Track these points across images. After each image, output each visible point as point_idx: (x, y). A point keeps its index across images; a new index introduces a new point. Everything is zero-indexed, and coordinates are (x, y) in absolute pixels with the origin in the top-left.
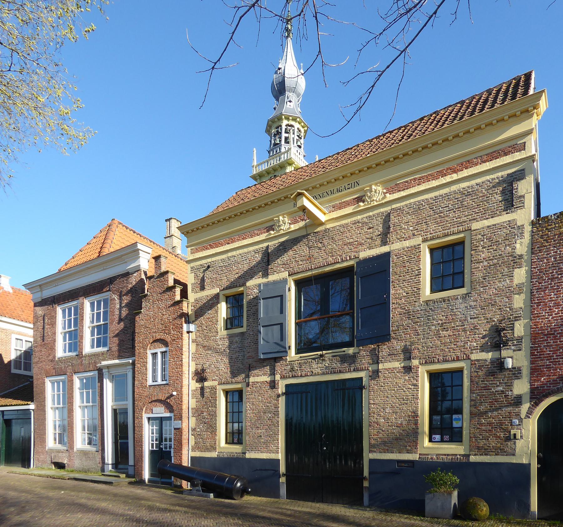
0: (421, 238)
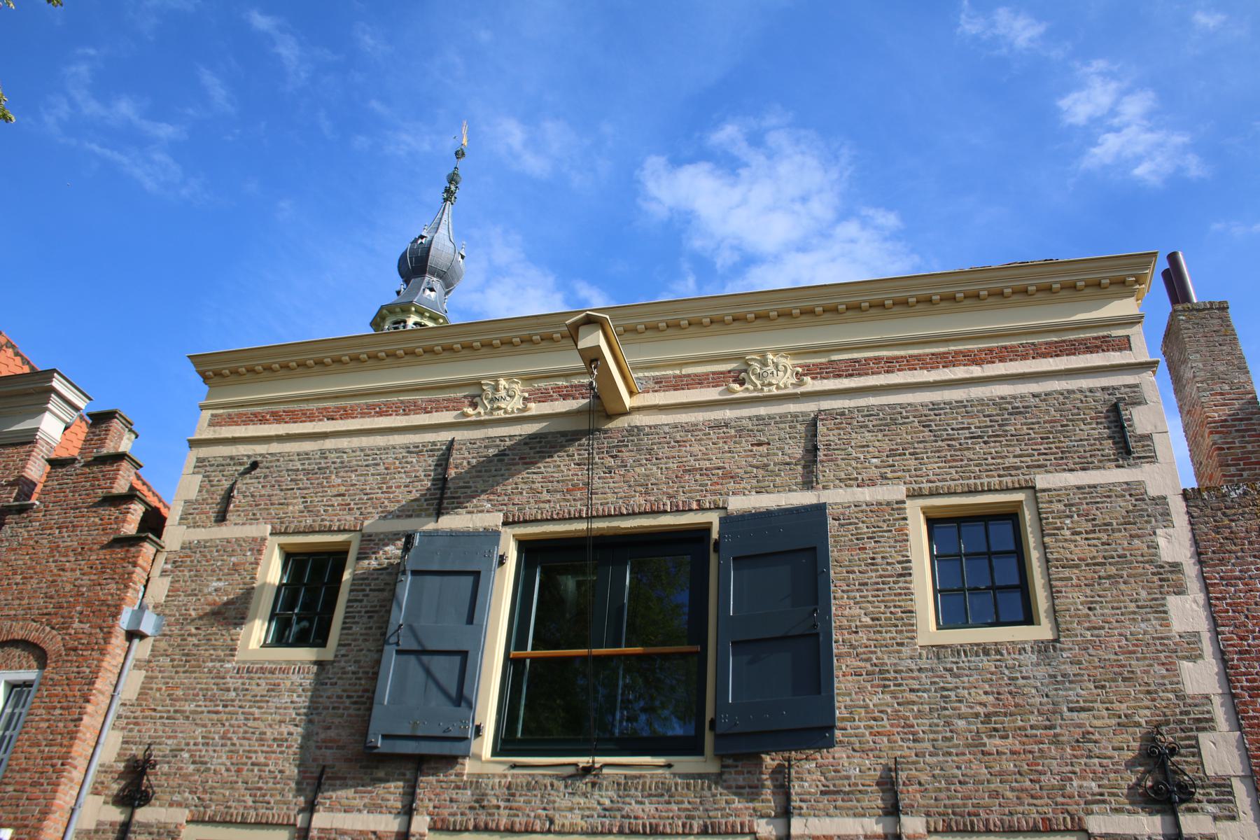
0: (903, 488)
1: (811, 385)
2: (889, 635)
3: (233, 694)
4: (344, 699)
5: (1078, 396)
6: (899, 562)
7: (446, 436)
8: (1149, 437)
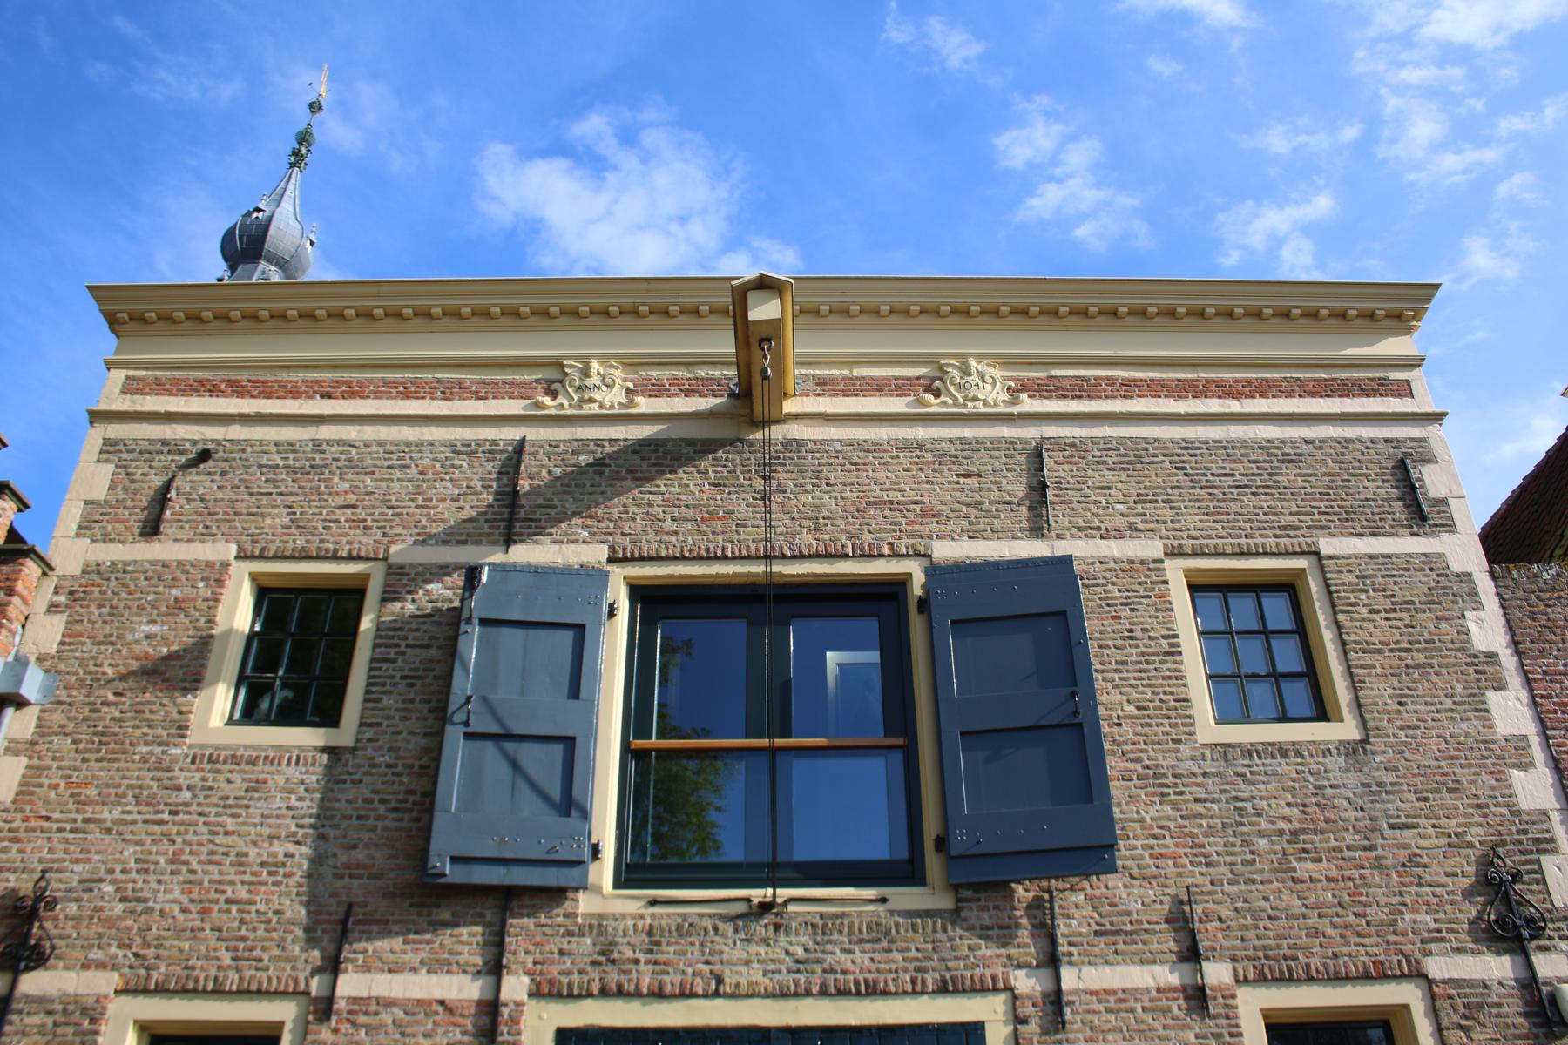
1: (1028, 404)
2: (1161, 729)
3: (186, 795)
4: (376, 804)
5: (1359, 446)
6: (1164, 637)
7: (512, 433)
8: (1444, 501)
